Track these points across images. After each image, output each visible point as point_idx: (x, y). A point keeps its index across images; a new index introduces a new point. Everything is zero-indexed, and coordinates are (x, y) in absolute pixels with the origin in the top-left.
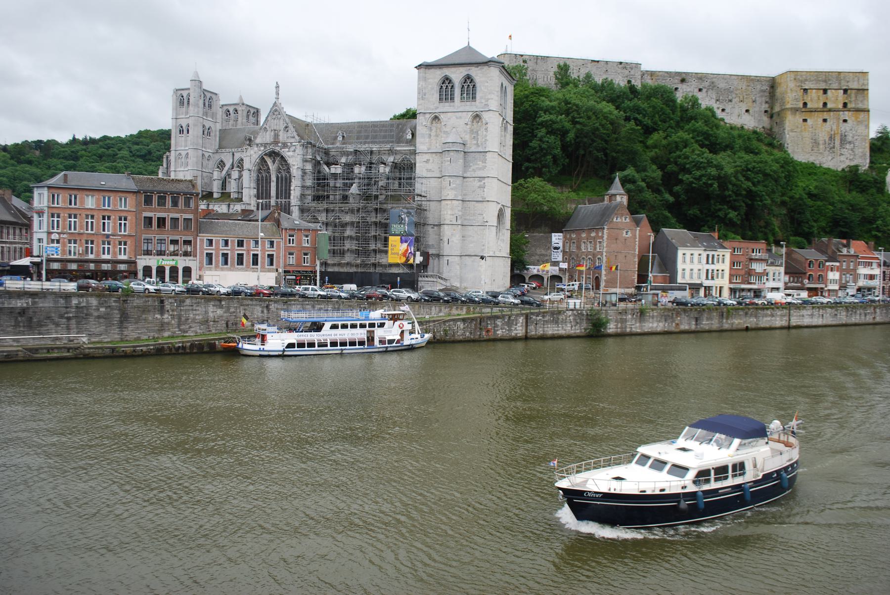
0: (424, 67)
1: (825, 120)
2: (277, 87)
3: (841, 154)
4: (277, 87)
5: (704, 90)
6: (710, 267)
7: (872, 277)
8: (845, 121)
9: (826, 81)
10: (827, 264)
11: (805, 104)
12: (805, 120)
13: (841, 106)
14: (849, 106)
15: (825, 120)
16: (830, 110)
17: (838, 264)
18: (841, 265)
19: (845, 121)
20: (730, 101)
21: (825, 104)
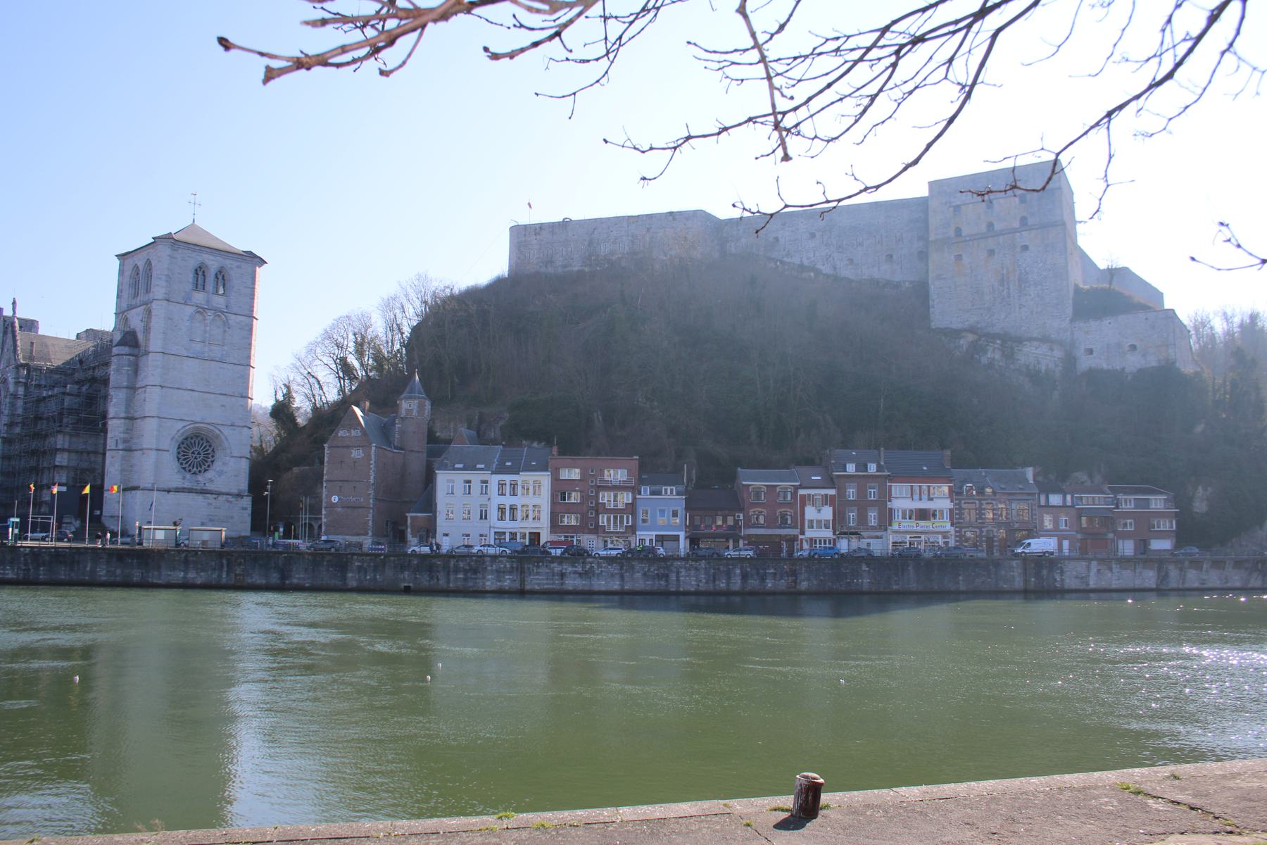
0: (122, 257)
1: (991, 253)
2: (14, 303)
3: (1021, 306)
4: (14, 303)
5: (818, 235)
6: (508, 501)
7: (923, 515)
8: (1025, 248)
9: (984, 188)
10: (801, 492)
11: (958, 232)
12: (959, 257)
13: (1016, 224)
14: (1030, 221)
15: (991, 253)
16: (1001, 233)
17: (832, 492)
18: (842, 492)
19: (1025, 248)
20: (861, 244)
21: (990, 225)
